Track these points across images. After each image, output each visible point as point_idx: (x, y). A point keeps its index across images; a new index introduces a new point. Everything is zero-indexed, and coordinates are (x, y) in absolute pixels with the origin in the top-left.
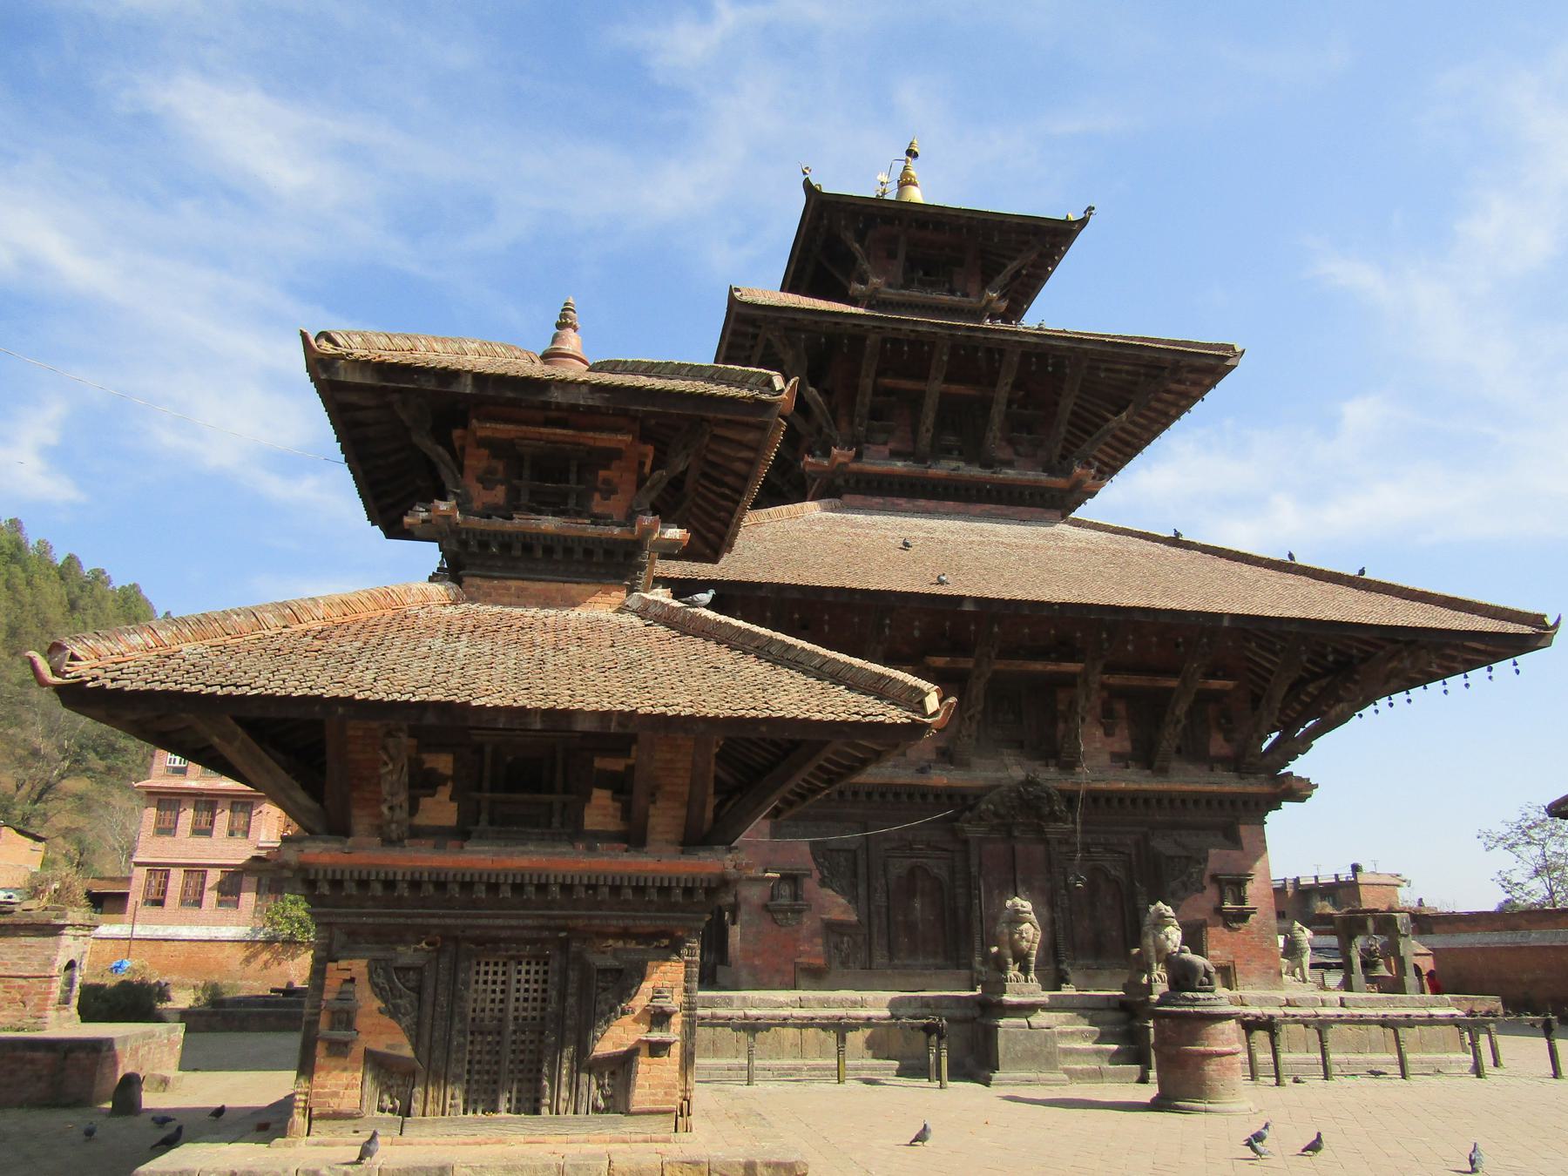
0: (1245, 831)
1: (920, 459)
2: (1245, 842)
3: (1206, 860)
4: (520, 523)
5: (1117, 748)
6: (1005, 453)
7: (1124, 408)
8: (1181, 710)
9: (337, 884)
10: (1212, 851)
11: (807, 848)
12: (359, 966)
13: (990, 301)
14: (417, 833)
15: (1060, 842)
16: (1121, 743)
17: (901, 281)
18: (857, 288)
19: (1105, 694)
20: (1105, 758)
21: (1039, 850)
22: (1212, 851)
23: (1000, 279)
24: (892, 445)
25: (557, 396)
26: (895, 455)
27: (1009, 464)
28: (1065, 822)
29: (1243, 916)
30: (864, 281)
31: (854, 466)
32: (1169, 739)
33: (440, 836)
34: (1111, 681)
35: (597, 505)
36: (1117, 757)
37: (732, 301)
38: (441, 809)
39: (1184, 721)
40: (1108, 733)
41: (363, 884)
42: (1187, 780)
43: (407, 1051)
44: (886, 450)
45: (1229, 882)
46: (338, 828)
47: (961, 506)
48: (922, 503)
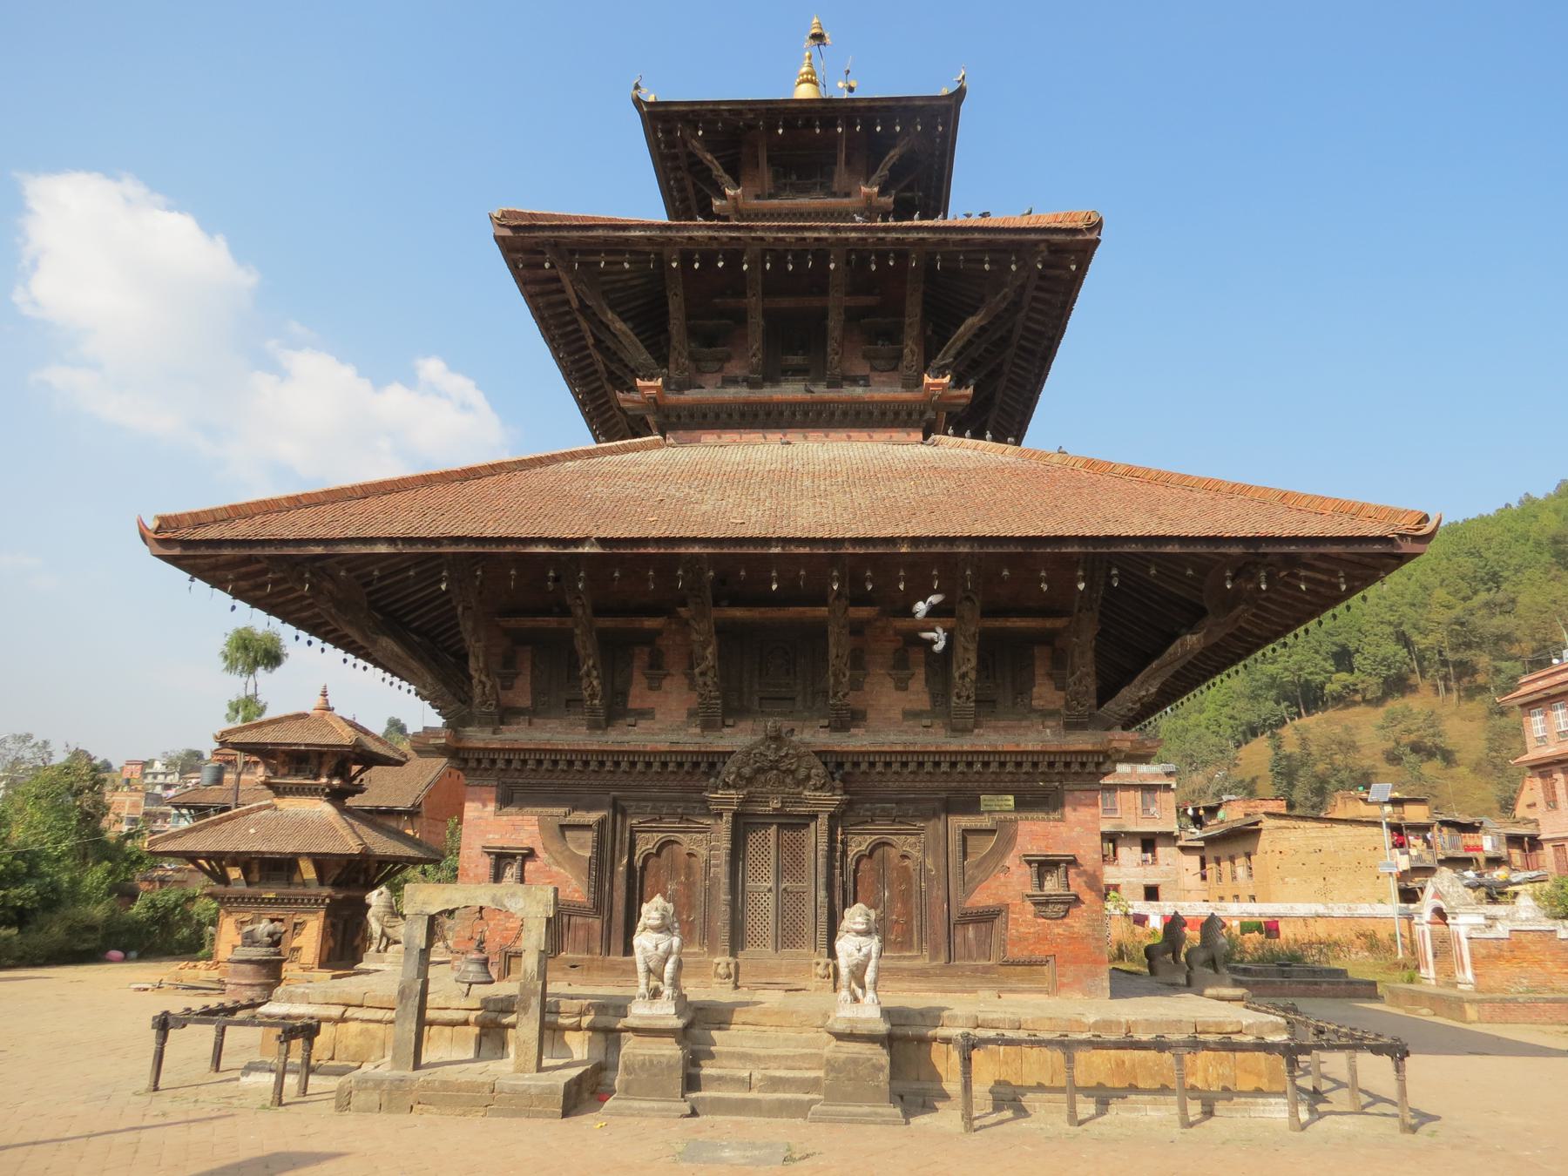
6: (861, 368)
16: (918, 694)
18: (717, 203)
20: (896, 714)
27: (854, 381)
30: (723, 196)
31: (672, 398)
36: (909, 715)
40: (902, 686)
45: (1041, 864)
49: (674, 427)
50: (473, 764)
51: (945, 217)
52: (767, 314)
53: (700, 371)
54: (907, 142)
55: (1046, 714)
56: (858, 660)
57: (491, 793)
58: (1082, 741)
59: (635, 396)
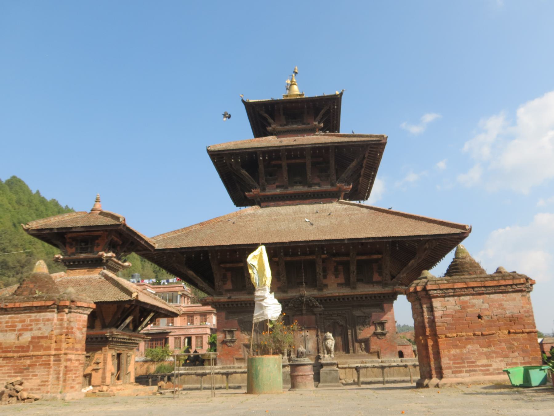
0: (386, 306)
1: (287, 188)
2: (386, 310)
3: (371, 316)
5: (339, 282)
6: (317, 180)
7: (353, 160)
8: (353, 268)
10: (374, 314)
11: (236, 322)
13: (315, 125)
15: (320, 314)
17: (285, 123)
18: (269, 129)
19: (335, 264)
21: (313, 317)
22: (374, 314)
23: (319, 118)
24: (277, 184)
25: (74, 230)
26: (278, 187)
28: (320, 308)
29: (383, 334)
30: (271, 126)
32: (353, 278)
34: (336, 259)
36: (340, 285)
37: (208, 151)
39: (356, 271)
40: (337, 276)
42: (363, 290)
44: (275, 186)
45: (378, 324)
47: (302, 201)
48: (288, 202)
49: (263, 202)
50: (218, 306)
51: (339, 132)
52: (289, 165)
53: (268, 184)
55: (378, 283)
56: (325, 270)
57: (223, 314)
58: (387, 290)
59: (251, 193)
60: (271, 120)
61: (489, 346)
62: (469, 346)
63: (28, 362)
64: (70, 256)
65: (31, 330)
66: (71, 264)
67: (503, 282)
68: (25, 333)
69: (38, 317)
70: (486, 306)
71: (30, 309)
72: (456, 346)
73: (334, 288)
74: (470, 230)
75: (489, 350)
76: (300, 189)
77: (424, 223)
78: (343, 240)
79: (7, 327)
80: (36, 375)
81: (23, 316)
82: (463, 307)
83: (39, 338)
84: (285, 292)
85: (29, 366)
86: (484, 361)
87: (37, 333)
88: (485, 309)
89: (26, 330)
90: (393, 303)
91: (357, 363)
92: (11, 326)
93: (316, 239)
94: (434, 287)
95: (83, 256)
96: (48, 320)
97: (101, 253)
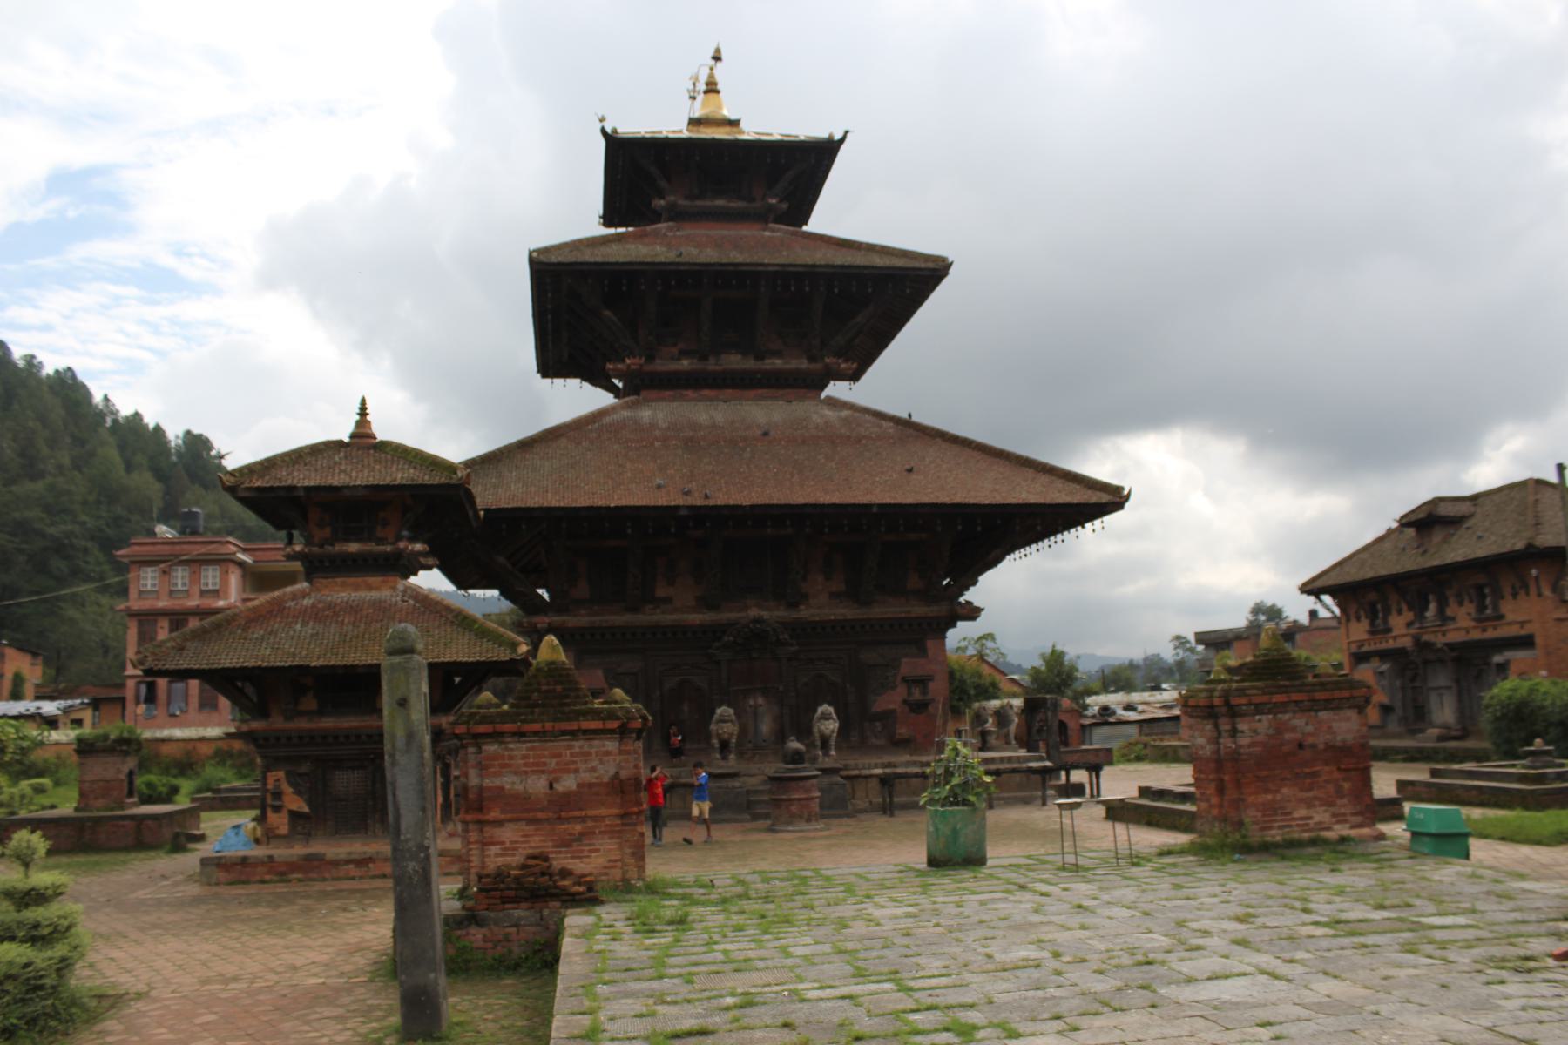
0: (930, 644)
2: (930, 653)
4: (339, 548)
9: (266, 739)
12: (281, 774)
14: (301, 714)
26: (684, 353)
27: (777, 354)
31: (649, 368)
33: (309, 714)
35: (380, 533)
36: (833, 595)
37: (532, 261)
38: (310, 703)
41: (278, 739)
43: (306, 809)
44: (675, 350)
46: (262, 711)
48: (706, 392)
54: (802, 166)
60: (663, 184)
61: (1311, 789)
62: (1285, 790)
63: (578, 828)
64: (322, 546)
65: (576, 771)
66: (318, 567)
67: (1337, 694)
68: (565, 776)
69: (586, 749)
70: (1310, 729)
71: (574, 734)
72: (1267, 791)
73: (822, 605)
74: (1127, 497)
75: (1311, 794)
76: (734, 361)
77: (1030, 473)
78: (866, 507)
79: (525, 765)
80: (597, 850)
81: (560, 745)
82: (1280, 729)
83: (590, 785)
84: (712, 607)
85: (582, 834)
86: (1302, 812)
87: (587, 777)
88: (1310, 734)
89: (568, 771)
90: (944, 637)
91: (876, 766)
92: (534, 764)
93: (812, 500)
94: (1244, 700)
95: (354, 547)
96: (608, 753)
97: (402, 545)
